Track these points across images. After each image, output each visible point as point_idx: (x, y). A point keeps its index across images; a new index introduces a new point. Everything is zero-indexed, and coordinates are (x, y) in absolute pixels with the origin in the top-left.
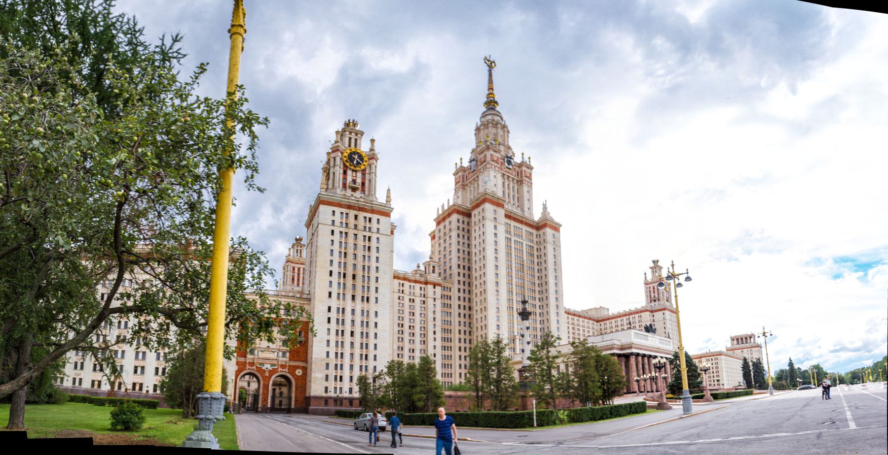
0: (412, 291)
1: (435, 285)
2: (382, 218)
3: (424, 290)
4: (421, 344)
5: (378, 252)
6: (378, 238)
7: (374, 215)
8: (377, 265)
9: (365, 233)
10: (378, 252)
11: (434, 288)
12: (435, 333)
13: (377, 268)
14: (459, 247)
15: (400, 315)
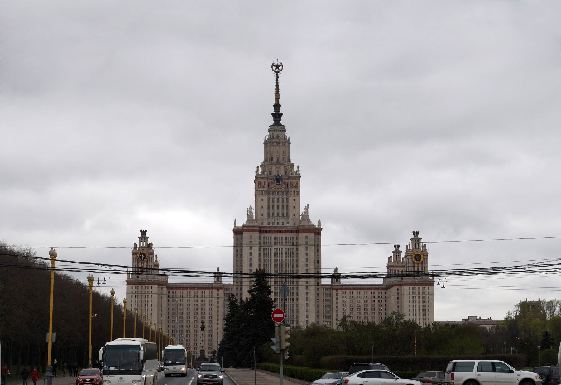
0: (203, 295)
1: (218, 289)
2: (153, 286)
3: (212, 293)
4: (209, 327)
5: (151, 302)
6: (151, 296)
7: (150, 285)
8: (152, 308)
9: (146, 294)
10: (151, 302)
11: (218, 291)
12: (218, 320)
13: (151, 309)
14: (238, 259)
15: (195, 311)
